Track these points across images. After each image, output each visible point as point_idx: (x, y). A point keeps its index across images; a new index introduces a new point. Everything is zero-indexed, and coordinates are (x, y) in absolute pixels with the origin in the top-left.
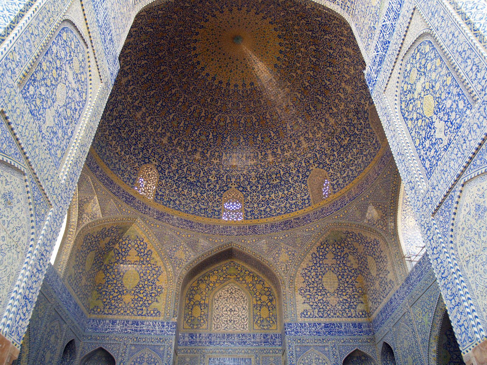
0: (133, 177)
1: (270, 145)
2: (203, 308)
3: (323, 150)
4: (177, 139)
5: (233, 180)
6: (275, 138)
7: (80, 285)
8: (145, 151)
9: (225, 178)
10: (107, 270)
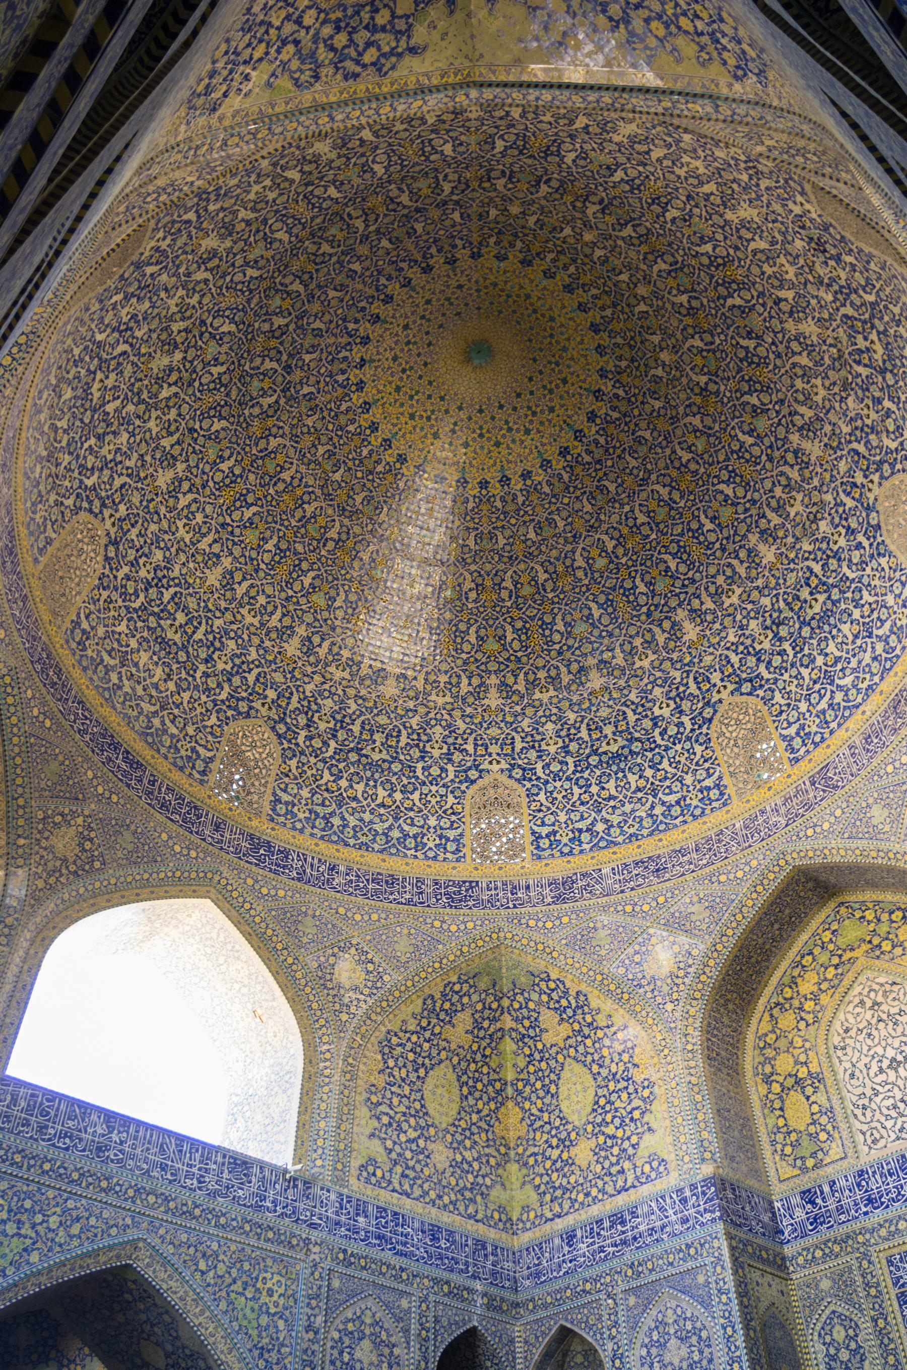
0: (451, 834)
1: (744, 521)
2: (809, 1090)
3: (859, 423)
4: (522, 676)
5: (716, 677)
6: (740, 492)
7: (427, 1171)
8: (457, 757)
10: (520, 1093)
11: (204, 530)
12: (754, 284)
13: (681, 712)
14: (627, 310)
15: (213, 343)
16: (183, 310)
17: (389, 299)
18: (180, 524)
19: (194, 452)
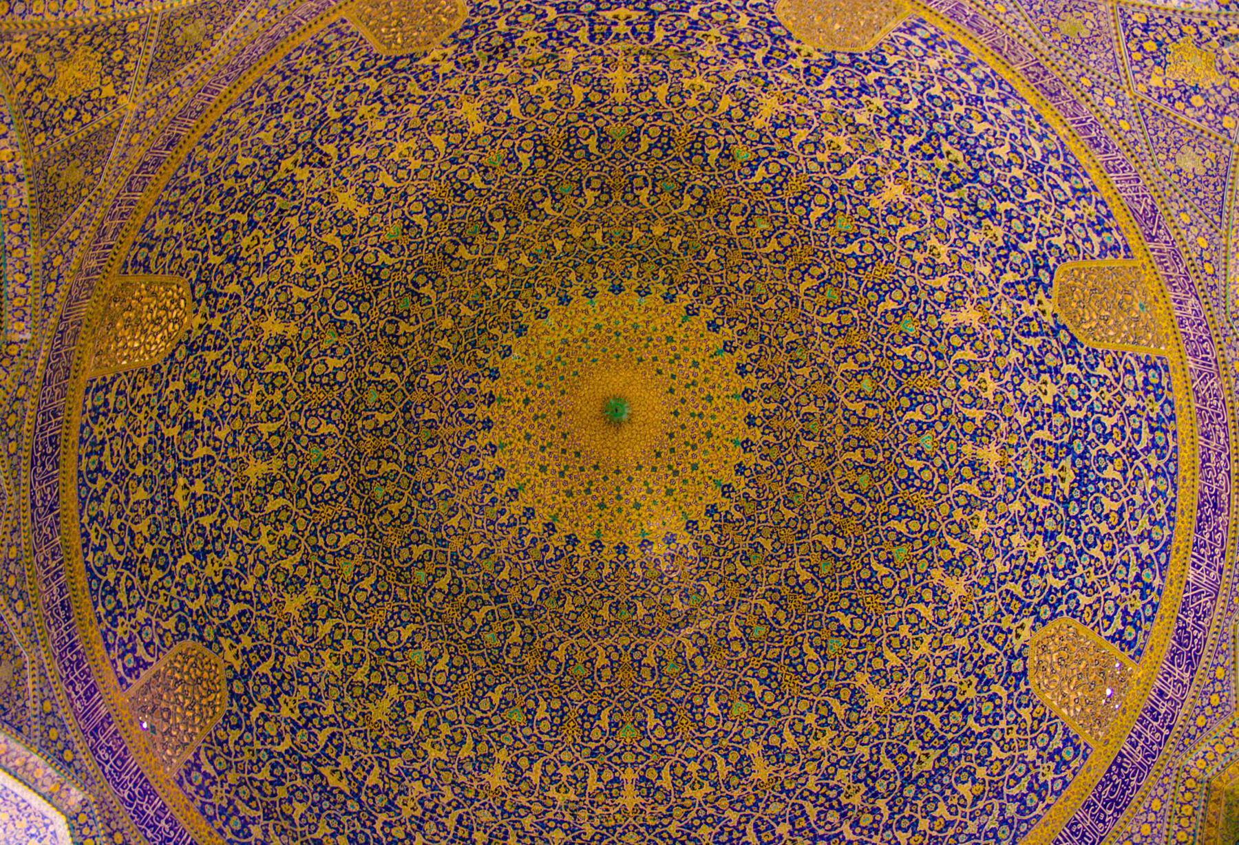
1: (854, 206)
4: (949, 539)
5: (1028, 309)
6: (820, 199)
8: (990, 671)
9: (1034, 342)
12: (568, 122)
13: (1057, 371)
14: (600, 252)
15: (410, 653)
16: (348, 661)
17: (499, 473)
18: (552, 793)
19: (500, 733)
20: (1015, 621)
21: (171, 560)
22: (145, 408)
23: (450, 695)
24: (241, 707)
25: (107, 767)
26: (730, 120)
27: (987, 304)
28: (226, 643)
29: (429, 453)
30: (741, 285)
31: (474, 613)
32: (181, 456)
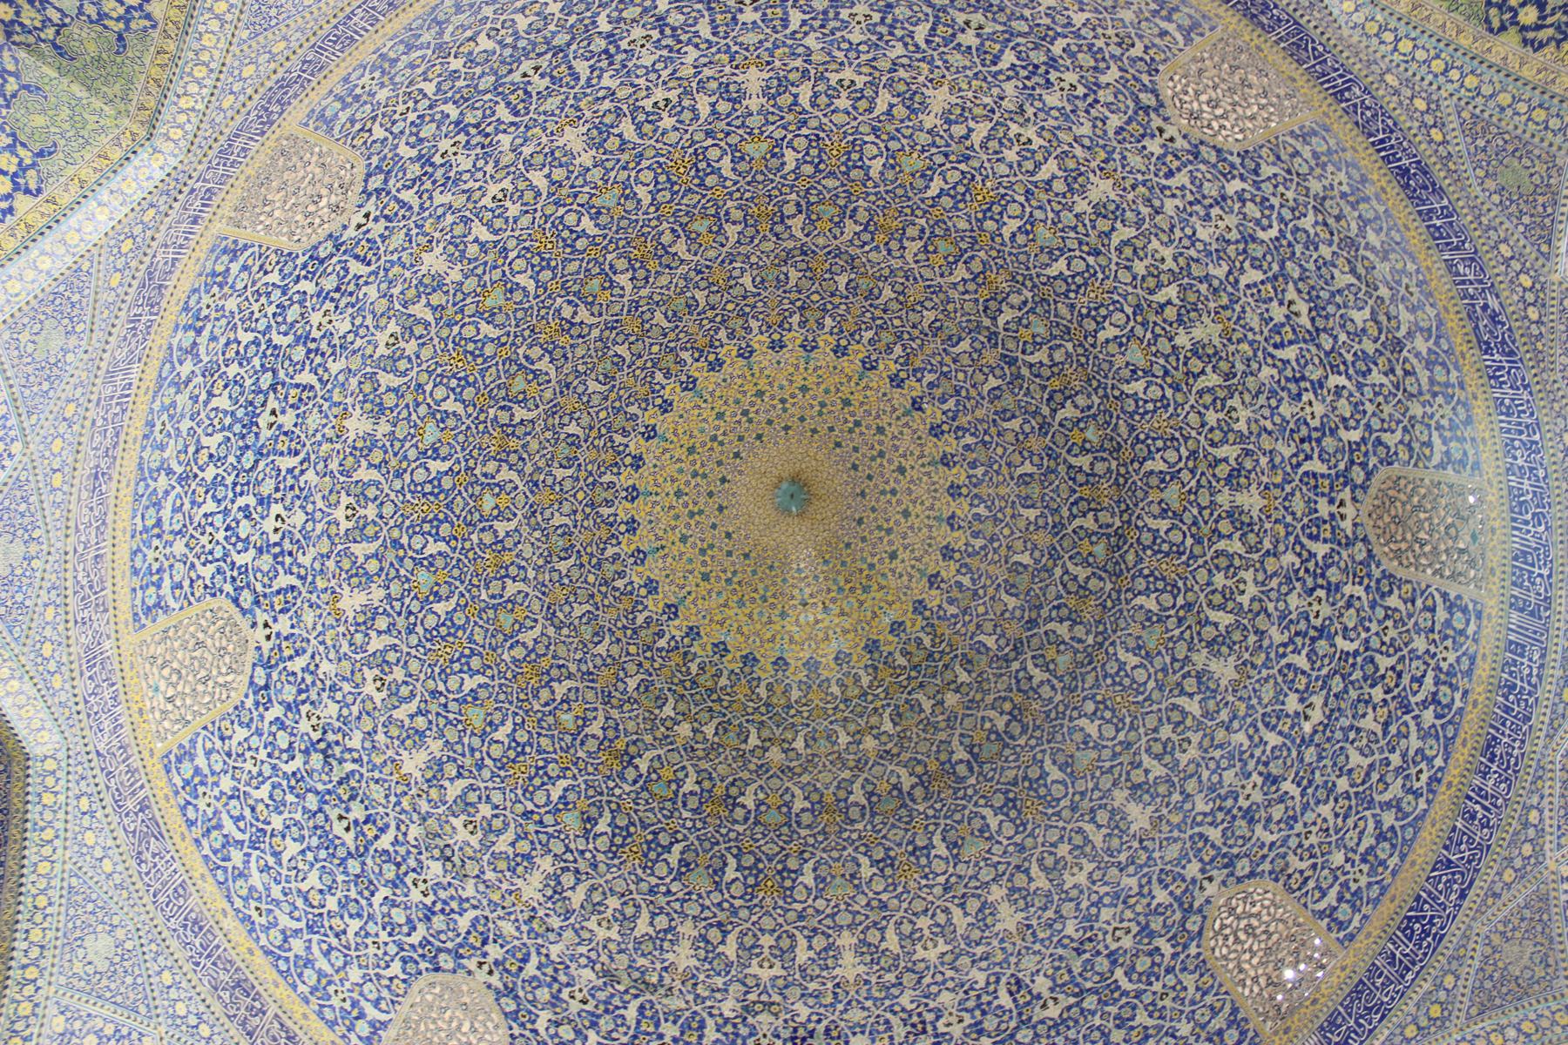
1: (460, 742)
4: (430, 318)
5: (283, 625)
6: (496, 751)
8: (415, 170)
9: (284, 580)
11: (993, 145)
13: (260, 551)
14: (757, 717)
15: (1142, 363)
17: (954, 491)
18: (1037, 142)
19: (1074, 228)
20: (368, 231)
21: (1359, 659)
22: (1306, 844)
23: (1116, 297)
24: (1366, 454)
25: (1545, 572)
26: (577, 871)
27: (330, 621)
28: (1347, 525)
29: (1025, 559)
30: (607, 639)
31: (1046, 361)
32: (1294, 753)
